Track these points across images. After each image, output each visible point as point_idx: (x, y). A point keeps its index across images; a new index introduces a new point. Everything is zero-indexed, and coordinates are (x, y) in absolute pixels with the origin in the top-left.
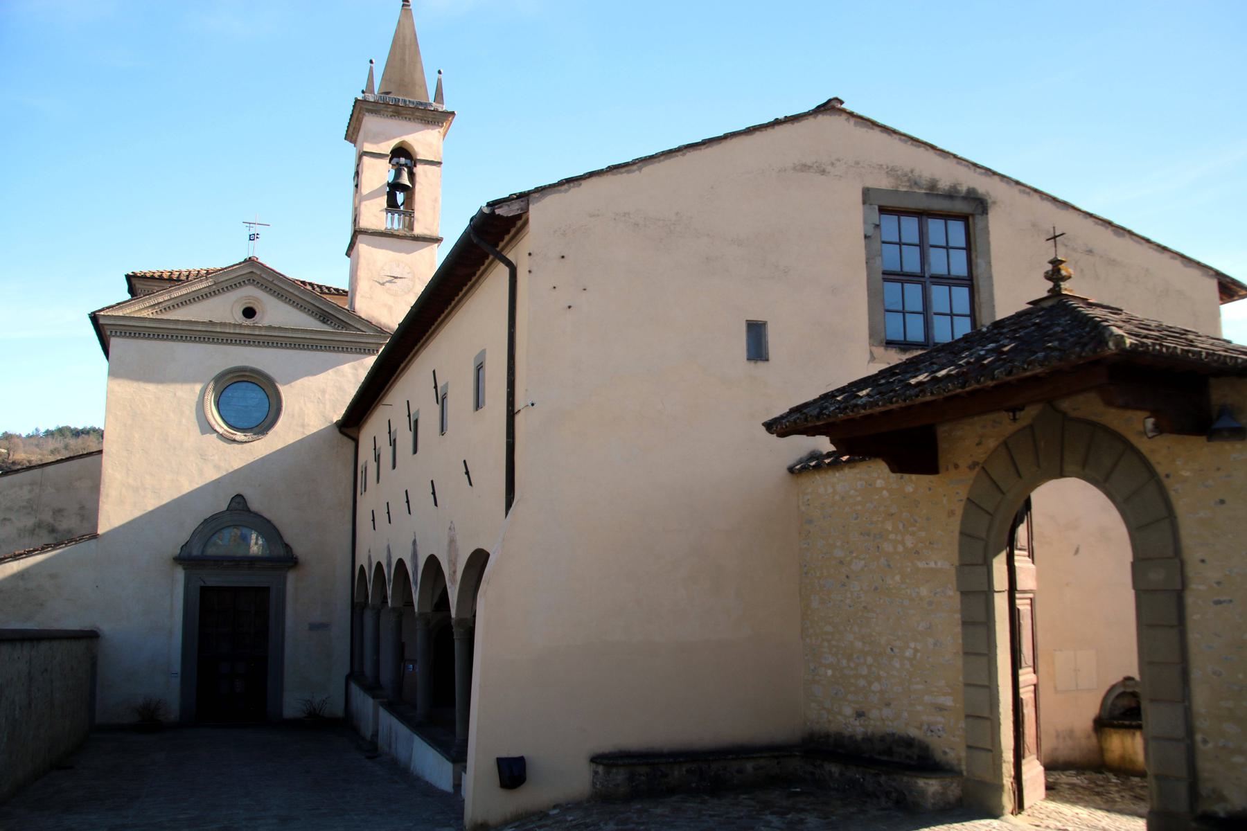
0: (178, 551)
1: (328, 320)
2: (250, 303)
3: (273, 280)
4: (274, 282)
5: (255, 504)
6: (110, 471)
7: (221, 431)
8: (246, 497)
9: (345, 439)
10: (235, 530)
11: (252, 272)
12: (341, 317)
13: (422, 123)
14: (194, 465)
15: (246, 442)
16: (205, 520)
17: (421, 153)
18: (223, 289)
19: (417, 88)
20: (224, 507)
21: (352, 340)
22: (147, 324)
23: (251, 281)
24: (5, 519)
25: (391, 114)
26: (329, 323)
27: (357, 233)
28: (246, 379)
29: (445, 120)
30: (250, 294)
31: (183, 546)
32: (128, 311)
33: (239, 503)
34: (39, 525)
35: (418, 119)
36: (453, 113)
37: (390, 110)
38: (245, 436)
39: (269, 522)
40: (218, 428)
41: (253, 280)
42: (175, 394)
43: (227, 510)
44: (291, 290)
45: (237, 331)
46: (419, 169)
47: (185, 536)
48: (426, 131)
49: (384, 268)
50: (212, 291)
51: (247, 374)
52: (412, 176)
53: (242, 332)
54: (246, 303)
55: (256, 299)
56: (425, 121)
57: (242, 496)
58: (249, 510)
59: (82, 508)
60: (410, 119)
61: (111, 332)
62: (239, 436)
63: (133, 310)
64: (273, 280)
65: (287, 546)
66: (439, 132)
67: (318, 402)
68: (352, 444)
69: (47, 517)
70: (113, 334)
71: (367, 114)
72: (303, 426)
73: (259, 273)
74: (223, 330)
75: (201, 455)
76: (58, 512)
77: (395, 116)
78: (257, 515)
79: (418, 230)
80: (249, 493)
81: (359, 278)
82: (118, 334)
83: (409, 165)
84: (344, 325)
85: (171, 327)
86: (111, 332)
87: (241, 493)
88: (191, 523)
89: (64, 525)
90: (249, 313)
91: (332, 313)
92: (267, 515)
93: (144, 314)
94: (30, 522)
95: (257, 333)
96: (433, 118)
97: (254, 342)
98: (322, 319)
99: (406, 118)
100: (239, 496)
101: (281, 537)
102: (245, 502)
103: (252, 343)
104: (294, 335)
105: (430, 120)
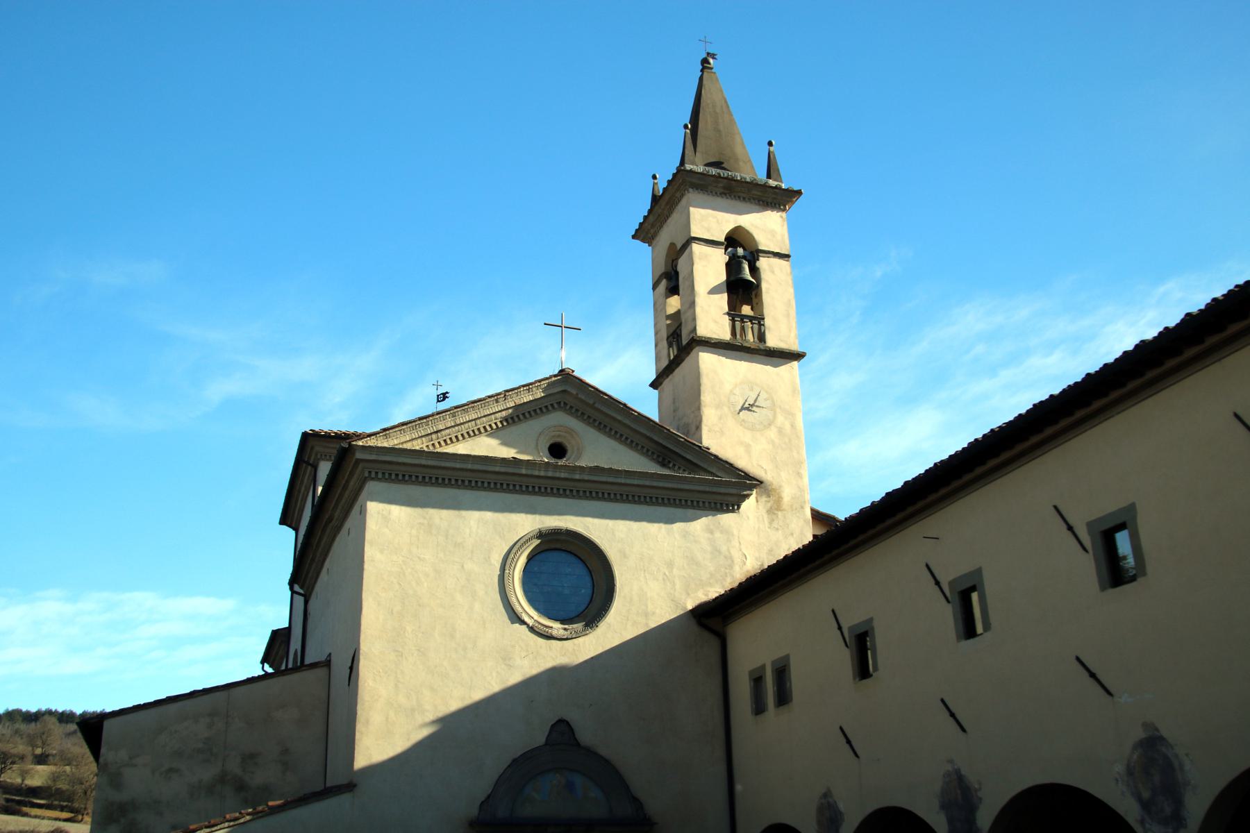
0: (474, 812)
1: (669, 462)
2: (559, 436)
3: (594, 403)
4: (596, 405)
5: (586, 734)
6: (371, 683)
7: (530, 622)
8: (572, 724)
9: (706, 634)
10: (558, 775)
11: (564, 391)
12: (688, 457)
13: (760, 205)
14: (494, 674)
15: (567, 639)
16: (515, 761)
17: (764, 243)
18: (523, 414)
19: (741, 163)
20: (540, 739)
21: (707, 489)
22: (423, 462)
23: (562, 404)
24: (171, 770)
25: (722, 190)
26: (671, 465)
27: (694, 344)
28: (558, 546)
29: (788, 202)
30: (559, 420)
31: (482, 802)
32: (396, 442)
33: (562, 731)
34: (222, 779)
35: (754, 199)
36: (799, 193)
37: (721, 185)
38: (565, 629)
39: (606, 762)
40: (526, 619)
41: (565, 403)
42: (463, 566)
43: (546, 744)
44: (619, 418)
45: (550, 474)
46: (763, 263)
47: (482, 787)
48: (769, 212)
49: (735, 392)
50: (531, 410)
51: (564, 538)
52: (754, 270)
53: (557, 475)
54: (554, 436)
55: (570, 431)
56: (763, 202)
57: (568, 723)
58: (578, 744)
59: (285, 751)
60: (744, 199)
61: (370, 472)
62: (557, 628)
63: (403, 440)
64: (594, 403)
65: (636, 801)
66: (782, 217)
67: (664, 579)
68: (714, 642)
69: (234, 766)
70: (373, 475)
71: (691, 190)
72: (646, 615)
73: (574, 392)
74: (529, 472)
75: (504, 659)
76: (250, 758)
77: (725, 194)
78: (590, 753)
79: (772, 341)
80: (574, 717)
81: (703, 403)
82: (380, 476)
83: (748, 258)
84: (694, 467)
85: (458, 466)
86: (370, 472)
87: (564, 718)
88: (494, 765)
89: (258, 778)
90: (557, 450)
91: (674, 449)
92: (603, 751)
93: (417, 445)
94: (207, 774)
95: (577, 477)
96: (775, 198)
97: (571, 491)
98: (660, 459)
99: (739, 197)
100: (562, 722)
101: (627, 787)
102: (572, 730)
103: (568, 492)
104: (628, 481)
105: (769, 200)
